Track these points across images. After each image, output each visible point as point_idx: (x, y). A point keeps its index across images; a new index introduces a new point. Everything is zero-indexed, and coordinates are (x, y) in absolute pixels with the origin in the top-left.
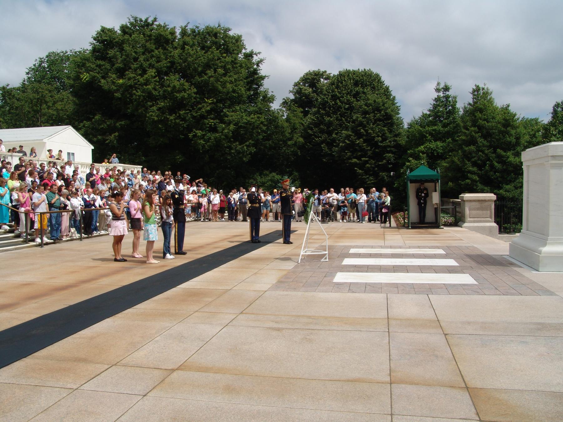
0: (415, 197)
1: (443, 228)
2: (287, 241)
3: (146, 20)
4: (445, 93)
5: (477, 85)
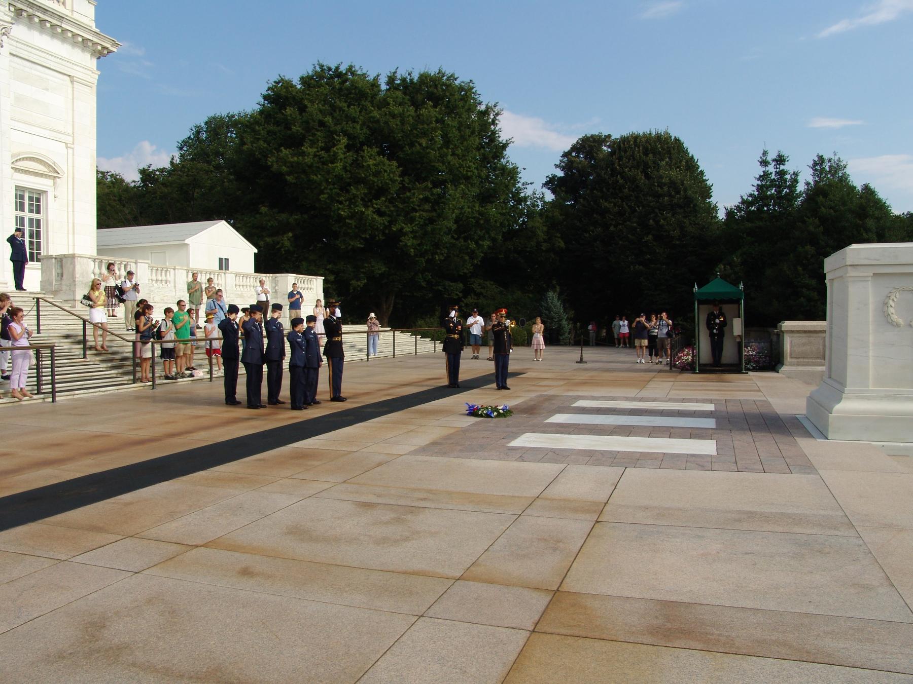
0: (706, 326)
1: (748, 373)
2: (502, 386)
3: (337, 68)
4: (778, 167)
5: (820, 155)
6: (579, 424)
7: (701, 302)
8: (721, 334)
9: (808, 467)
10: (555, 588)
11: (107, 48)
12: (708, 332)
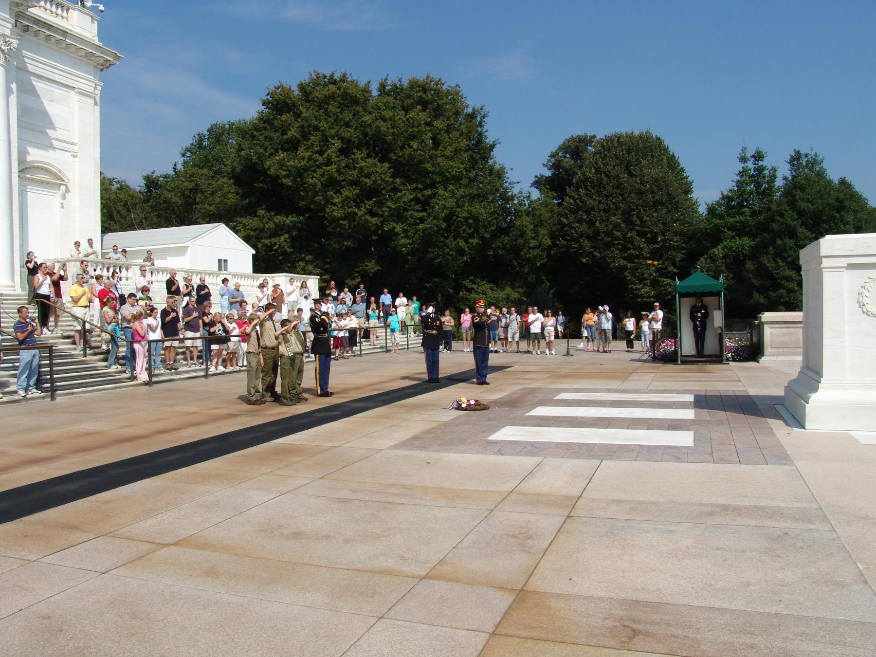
3: (332, 75)
4: (757, 162)
5: (797, 150)
6: (559, 417)
7: (682, 295)
8: (704, 326)
9: (783, 458)
10: (520, 587)
11: (110, 61)
12: (692, 323)
